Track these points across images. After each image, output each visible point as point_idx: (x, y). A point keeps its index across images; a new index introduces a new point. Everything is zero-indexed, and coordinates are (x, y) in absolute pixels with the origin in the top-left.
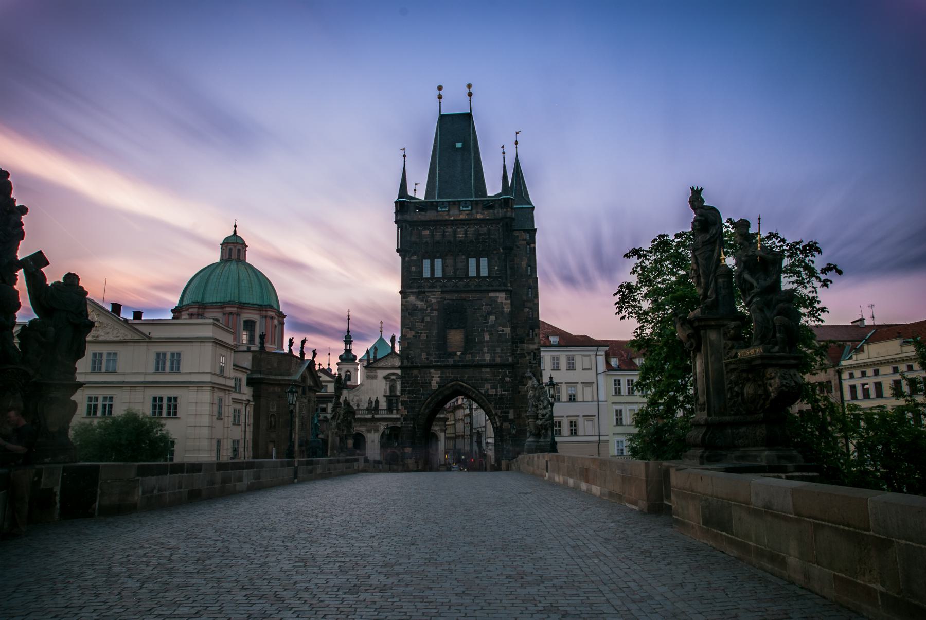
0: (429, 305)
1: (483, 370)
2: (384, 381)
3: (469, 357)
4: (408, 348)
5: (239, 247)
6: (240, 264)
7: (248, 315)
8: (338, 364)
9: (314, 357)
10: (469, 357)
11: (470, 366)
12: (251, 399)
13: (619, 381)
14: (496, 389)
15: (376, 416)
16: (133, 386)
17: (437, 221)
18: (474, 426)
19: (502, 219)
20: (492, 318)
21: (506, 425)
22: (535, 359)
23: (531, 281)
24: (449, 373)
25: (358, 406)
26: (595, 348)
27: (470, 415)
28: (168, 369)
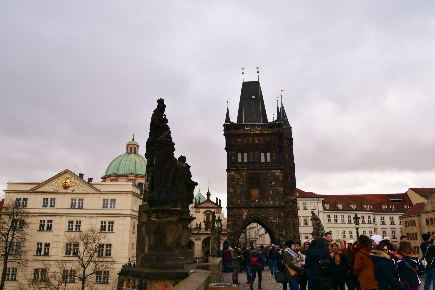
0: (242, 176)
1: (269, 209)
2: (204, 214)
3: (262, 203)
10: (262, 203)
15: (200, 232)
16: (91, 215)
18: (247, 238)
20: (273, 183)
22: (294, 204)
26: (317, 199)
28: (109, 207)
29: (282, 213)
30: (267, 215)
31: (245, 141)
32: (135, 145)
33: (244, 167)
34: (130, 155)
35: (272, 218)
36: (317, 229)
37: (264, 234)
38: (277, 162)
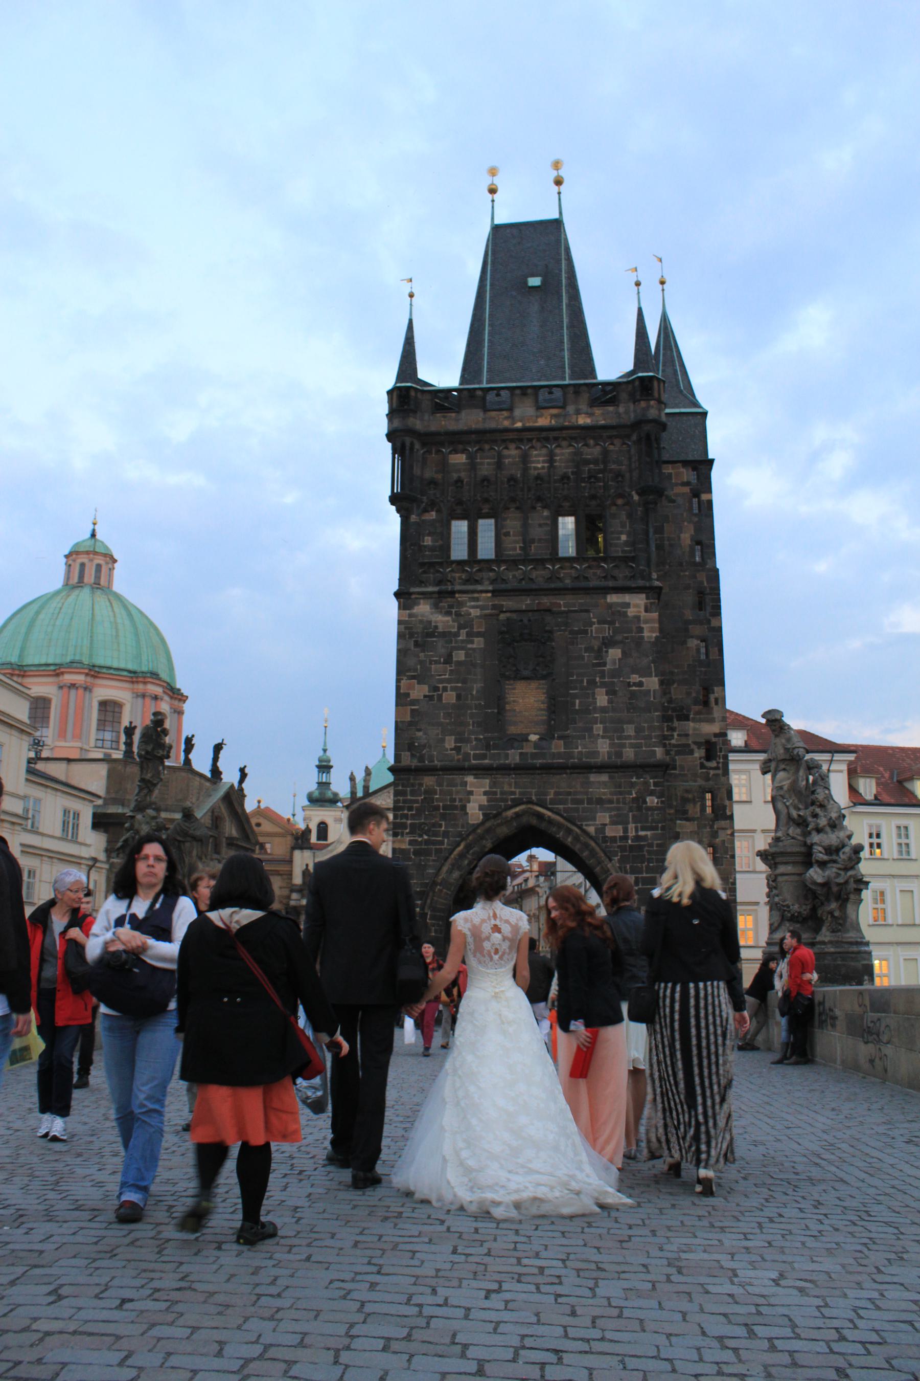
1: (593, 778)
4: (410, 724)
5: (99, 560)
6: (99, 592)
7: (106, 691)
9: (242, 780)
10: (557, 746)
12: (102, 856)
14: (625, 823)
19: (637, 424)
20: (615, 653)
23: (702, 577)
24: (510, 785)
29: (652, 793)
30: (581, 802)
31: (486, 467)
32: (96, 553)
33: (477, 582)
34: (76, 592)
38: (633, 559)
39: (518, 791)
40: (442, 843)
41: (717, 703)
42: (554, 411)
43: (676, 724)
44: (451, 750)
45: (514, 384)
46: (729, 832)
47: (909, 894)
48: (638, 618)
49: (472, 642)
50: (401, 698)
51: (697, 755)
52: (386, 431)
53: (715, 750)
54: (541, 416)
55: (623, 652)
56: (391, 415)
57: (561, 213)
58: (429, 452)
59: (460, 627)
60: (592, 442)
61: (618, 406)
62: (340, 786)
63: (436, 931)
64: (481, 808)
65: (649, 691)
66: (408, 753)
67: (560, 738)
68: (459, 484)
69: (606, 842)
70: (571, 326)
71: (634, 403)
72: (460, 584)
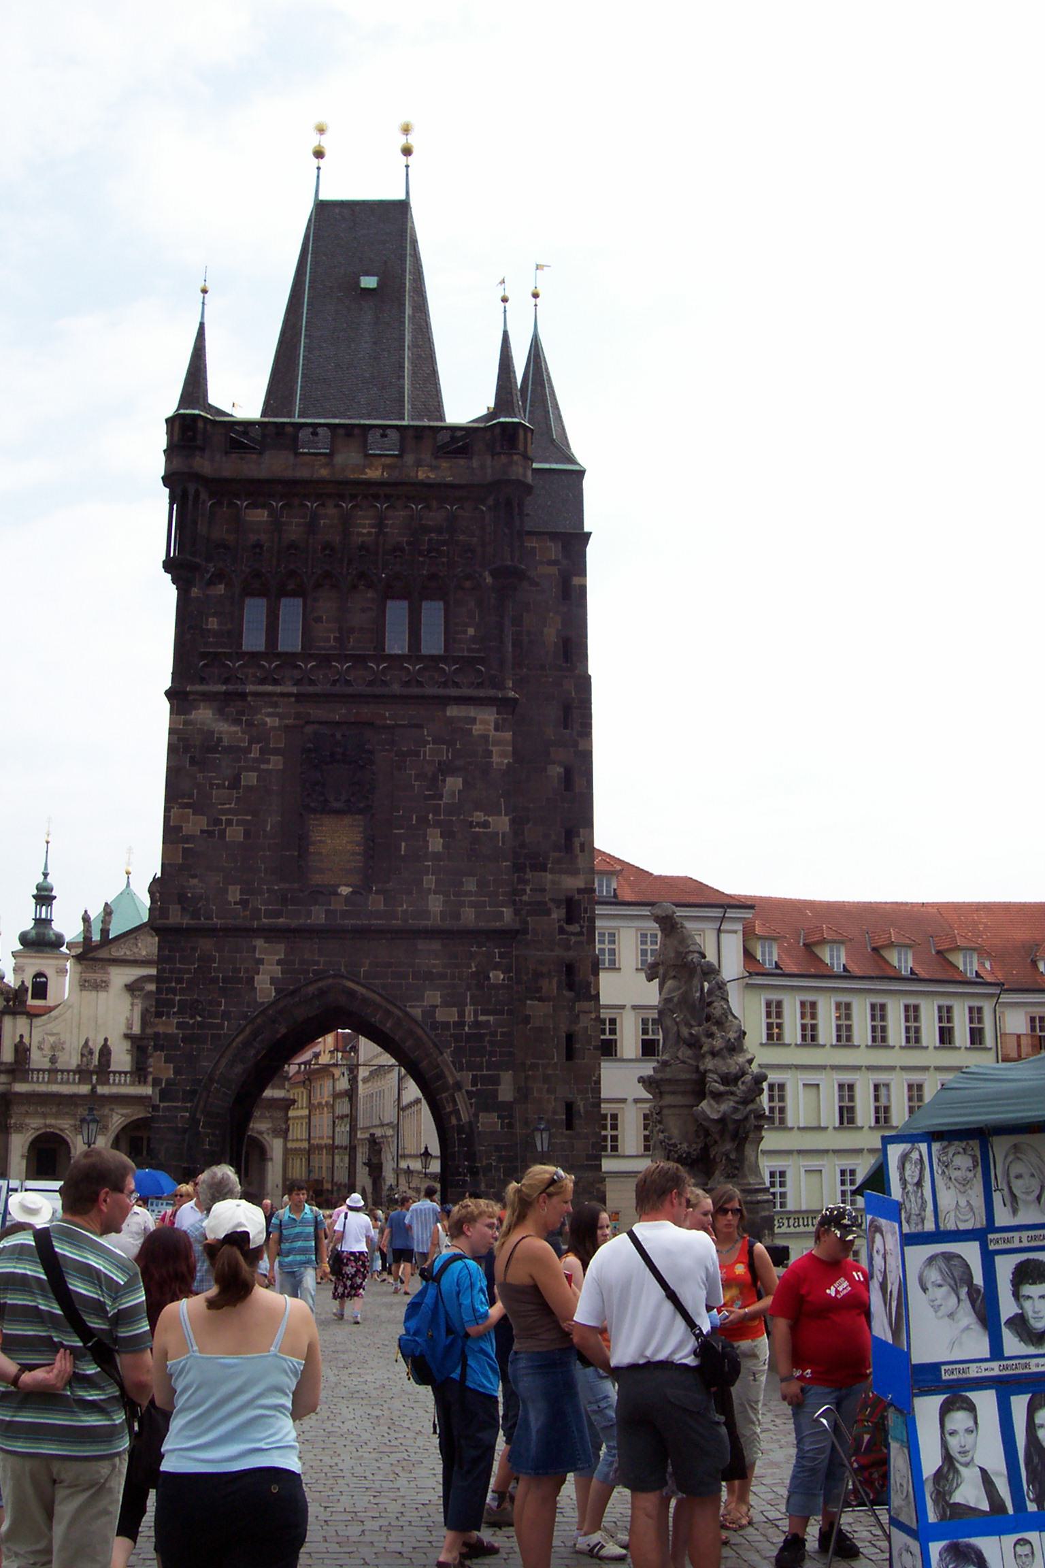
1: (422, 945)
2: (127, 999)
8: (14, 954)
10: (376, 903)
11: (381, 932)
13: (779, 1004)
15: (101, 1090)
17: (295, 482)
18: (361, 1124)
20: (453, 784)
21: (488, 1121)
25: (53, 1060)
26: (717, 913)
27: (351, 1094)
29: (496, 967)
31: (294, 529)
33: (276, 682)
35: (433, 997)
36: (694, 1044)
37: (418, 1101)
38: (482, 661)
39: (322, 960)
40: (220, 1026)
41: (582, 850)
42: (388, 461)
43: (529, 876)
44: (235, 903)
45: (337, 421)
46: (593, 1016)
47: (814, 1090)
48: (485, 738)
49: (268, 762)
50: (171, 833)
51: (554, 916)
52: (162, 473)
53: (578, 911)
54: (370, 466)
55: (465, 782)
56: (168, 452)
57: (407, 193)
58: (219, 503)
59: (250, 743)
60: (434, 504)
61: (471, 458)
62: (67, 925)
63: (210, 1144)
64: (273, 981)
65: (497, 834)
66: (178, 907)
67: (377, 892)
68: (258, 550)
69: (436, 1029)
70: (415, 345)
71: (493, 456)
72: (253, 683)
